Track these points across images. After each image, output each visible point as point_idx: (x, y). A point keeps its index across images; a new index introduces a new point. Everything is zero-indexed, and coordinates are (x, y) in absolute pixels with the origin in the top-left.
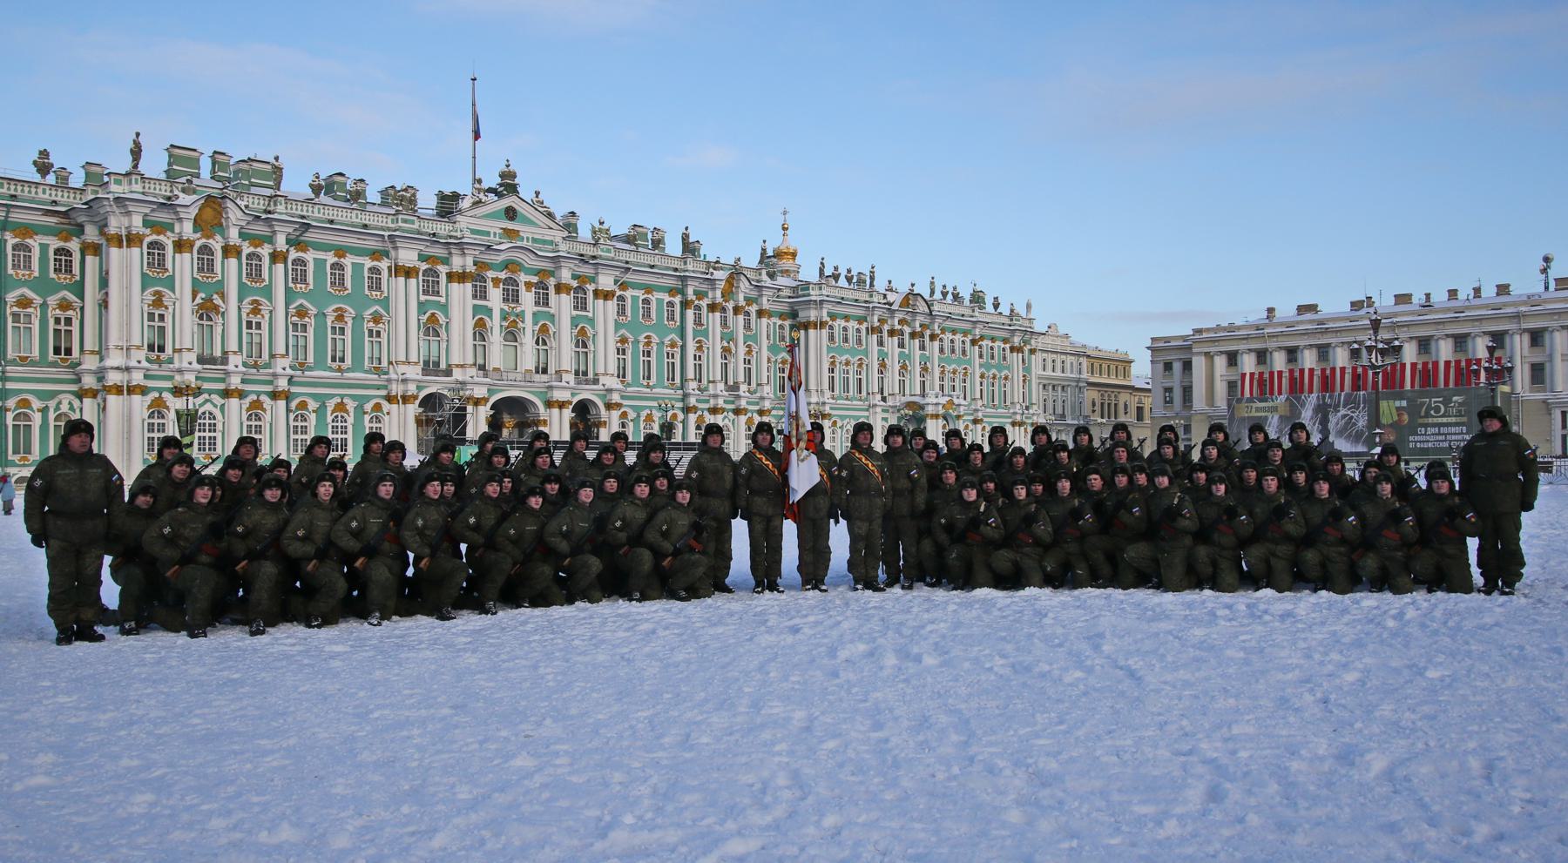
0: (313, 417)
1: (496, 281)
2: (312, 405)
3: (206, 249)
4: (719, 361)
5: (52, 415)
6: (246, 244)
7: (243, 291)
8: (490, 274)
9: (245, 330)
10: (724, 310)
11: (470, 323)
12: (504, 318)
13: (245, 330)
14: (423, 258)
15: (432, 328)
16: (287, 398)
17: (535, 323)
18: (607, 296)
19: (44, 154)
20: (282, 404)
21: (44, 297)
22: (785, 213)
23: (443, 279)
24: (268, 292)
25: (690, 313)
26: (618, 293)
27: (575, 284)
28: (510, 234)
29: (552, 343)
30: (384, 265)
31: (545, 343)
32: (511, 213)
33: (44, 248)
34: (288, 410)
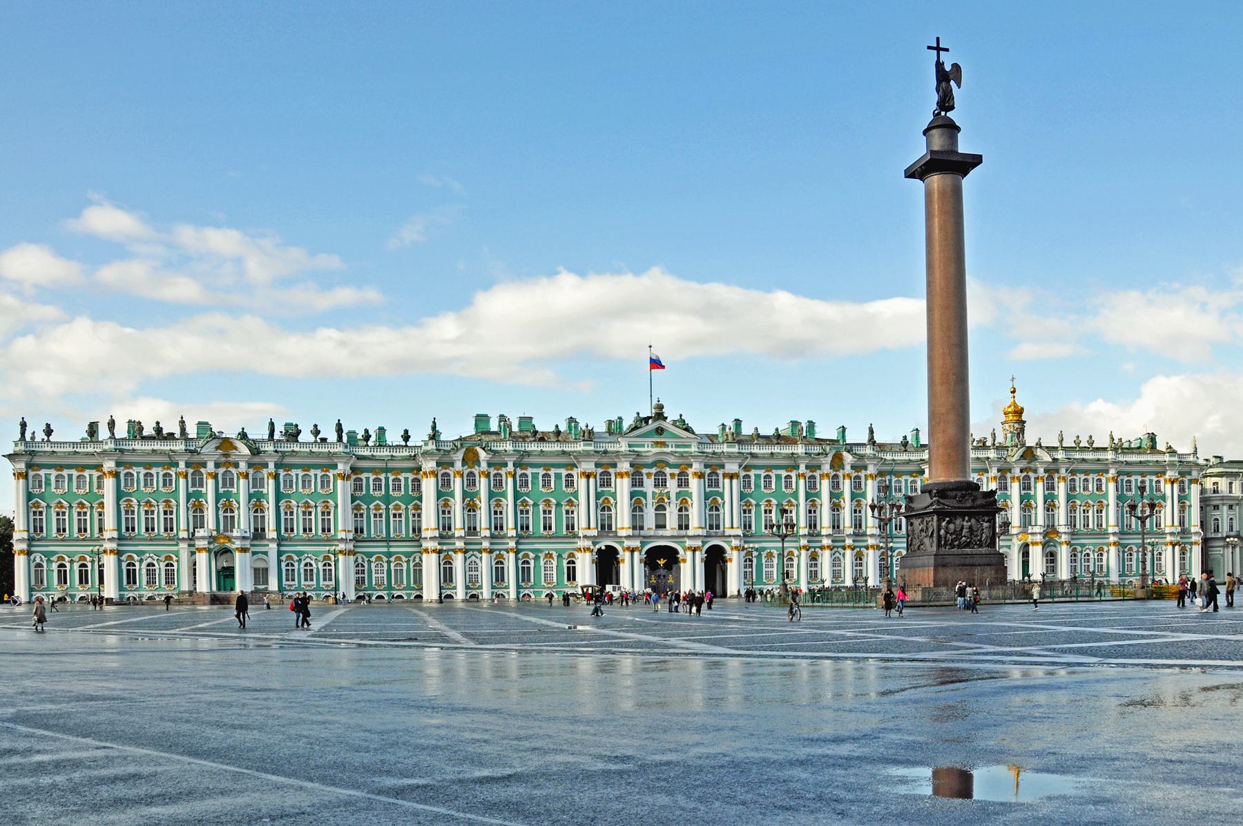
0: (532, 562)
1: (649, 475)
2: (532, 555)
3: (471, 474)
5: (412, 564)
7: (491, 495)
8: (645, 471)
10: (836, 476)
16: (517, 552)
18: (732, 477)
19: (406, 432)
20: (512, 555)
21: (406, 505)
22: (1013, 379)
26: (743, 473)
27: (708, 471)
30: (574, 472)
32: (660, 431)
33: (406, 479)
34: (517, 559)
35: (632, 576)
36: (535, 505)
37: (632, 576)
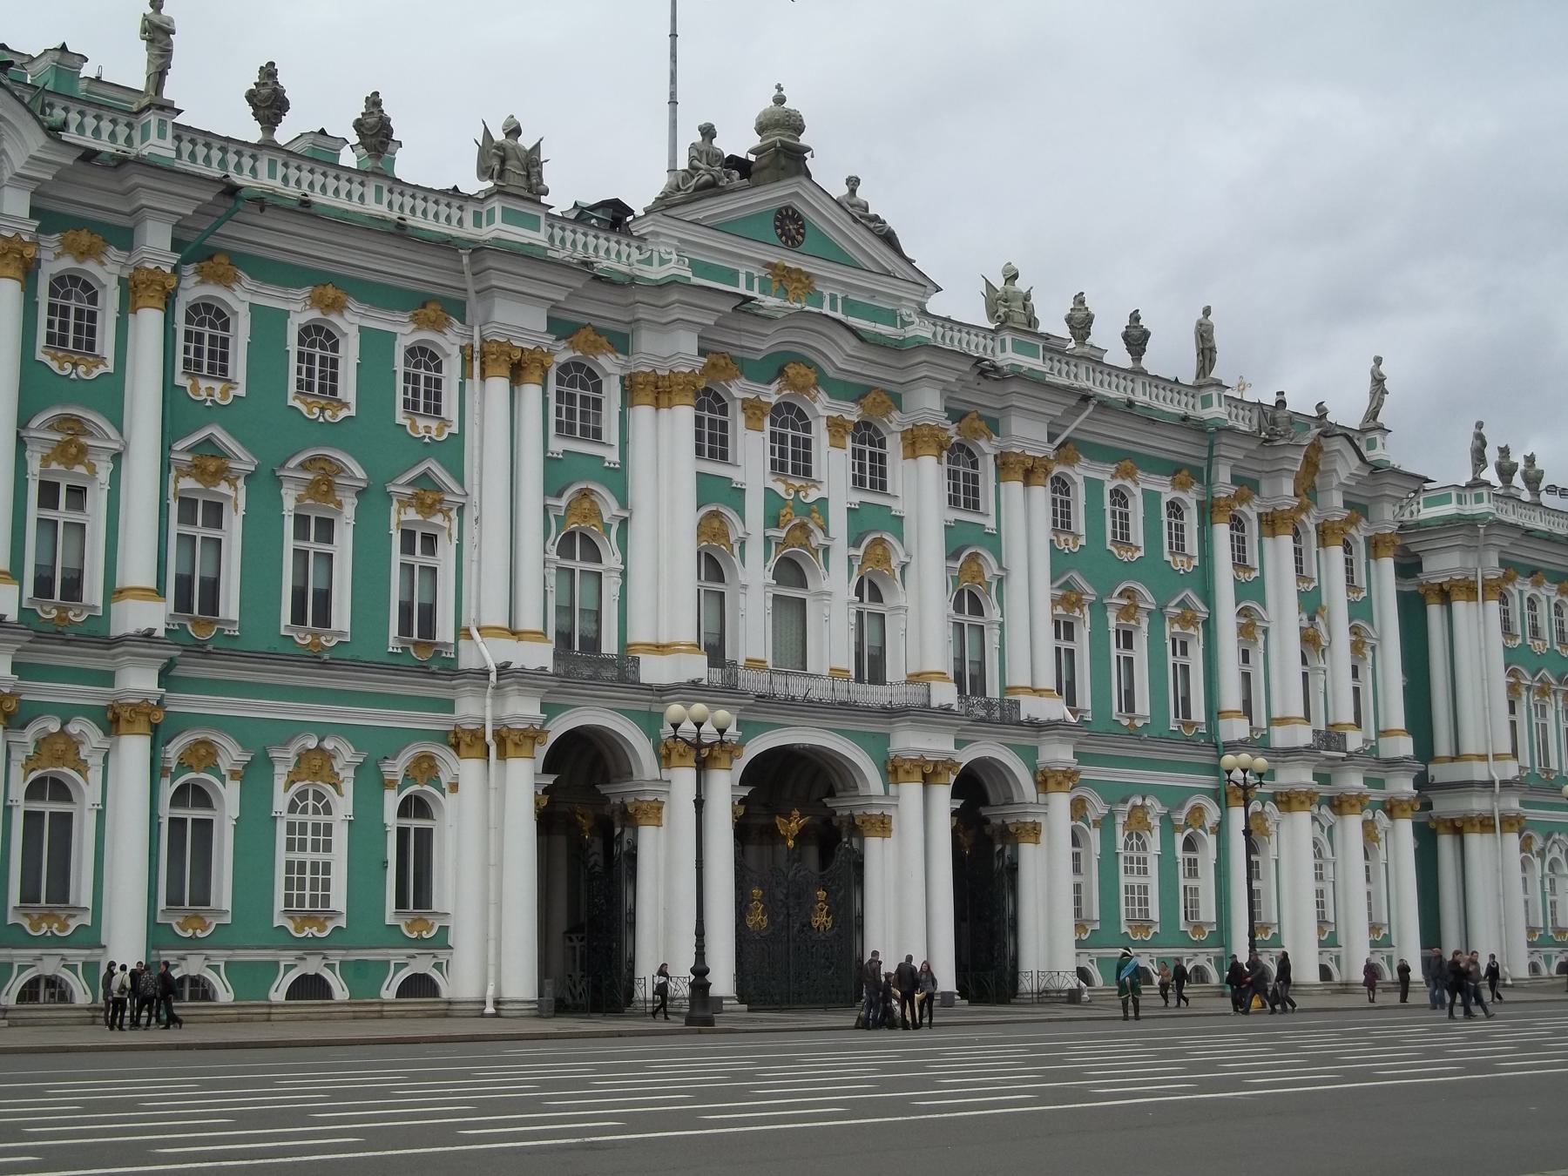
1: (753, 409)
2: (231, 754)
4: (1296, 668)
6: (52, 241)
8: (739, 390)
9: (33, 512)
11: (686, 516)
12: (773, 520)
13: (33, 512)
14: (560, 327)
15: (582, 537)
16: (159, 736)
17: (855, 542)
23: (612, 394)
24: (110, 396)
25: (1222, 533)
28: (783, 279)
29: (896, 597)
30: (449, 343)
31: (876, 596)
34: (157, 770)
35: (685, 898)
36: (264, 483)
37: (685, 898)
